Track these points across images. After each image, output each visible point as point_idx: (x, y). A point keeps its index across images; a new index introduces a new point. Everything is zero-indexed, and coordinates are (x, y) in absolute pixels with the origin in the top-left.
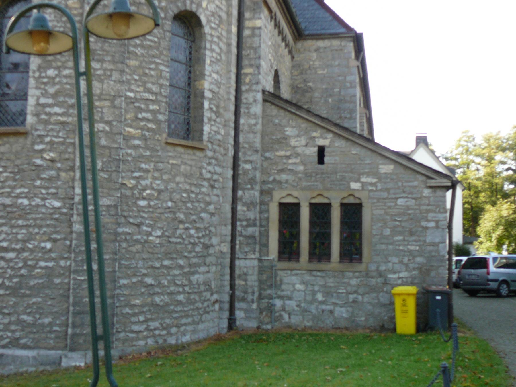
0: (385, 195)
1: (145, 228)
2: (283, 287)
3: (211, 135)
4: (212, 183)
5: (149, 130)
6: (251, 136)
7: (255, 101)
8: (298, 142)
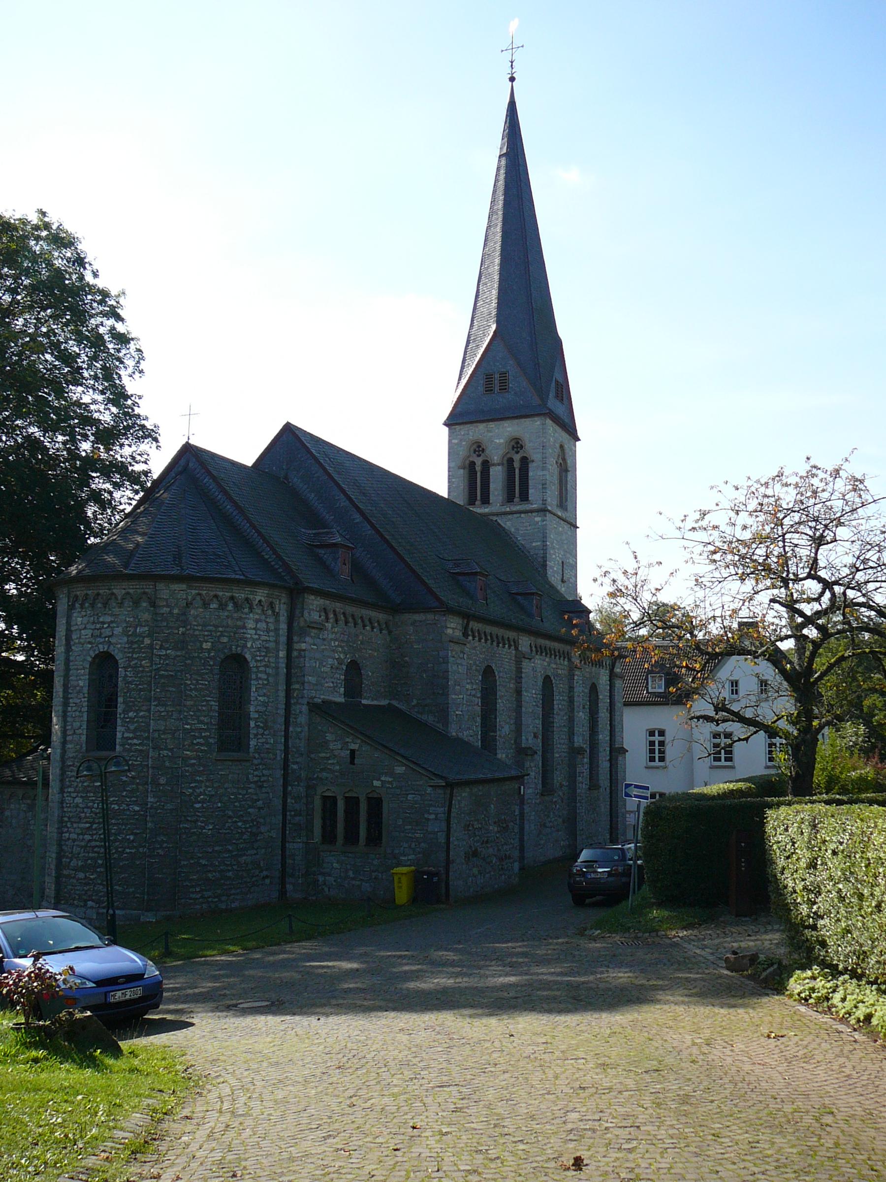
0: (398, 791)
2: (325, 865)
4: (260, 784)
6: (297, 741)
7: (301, 712)
8: (335, 746)
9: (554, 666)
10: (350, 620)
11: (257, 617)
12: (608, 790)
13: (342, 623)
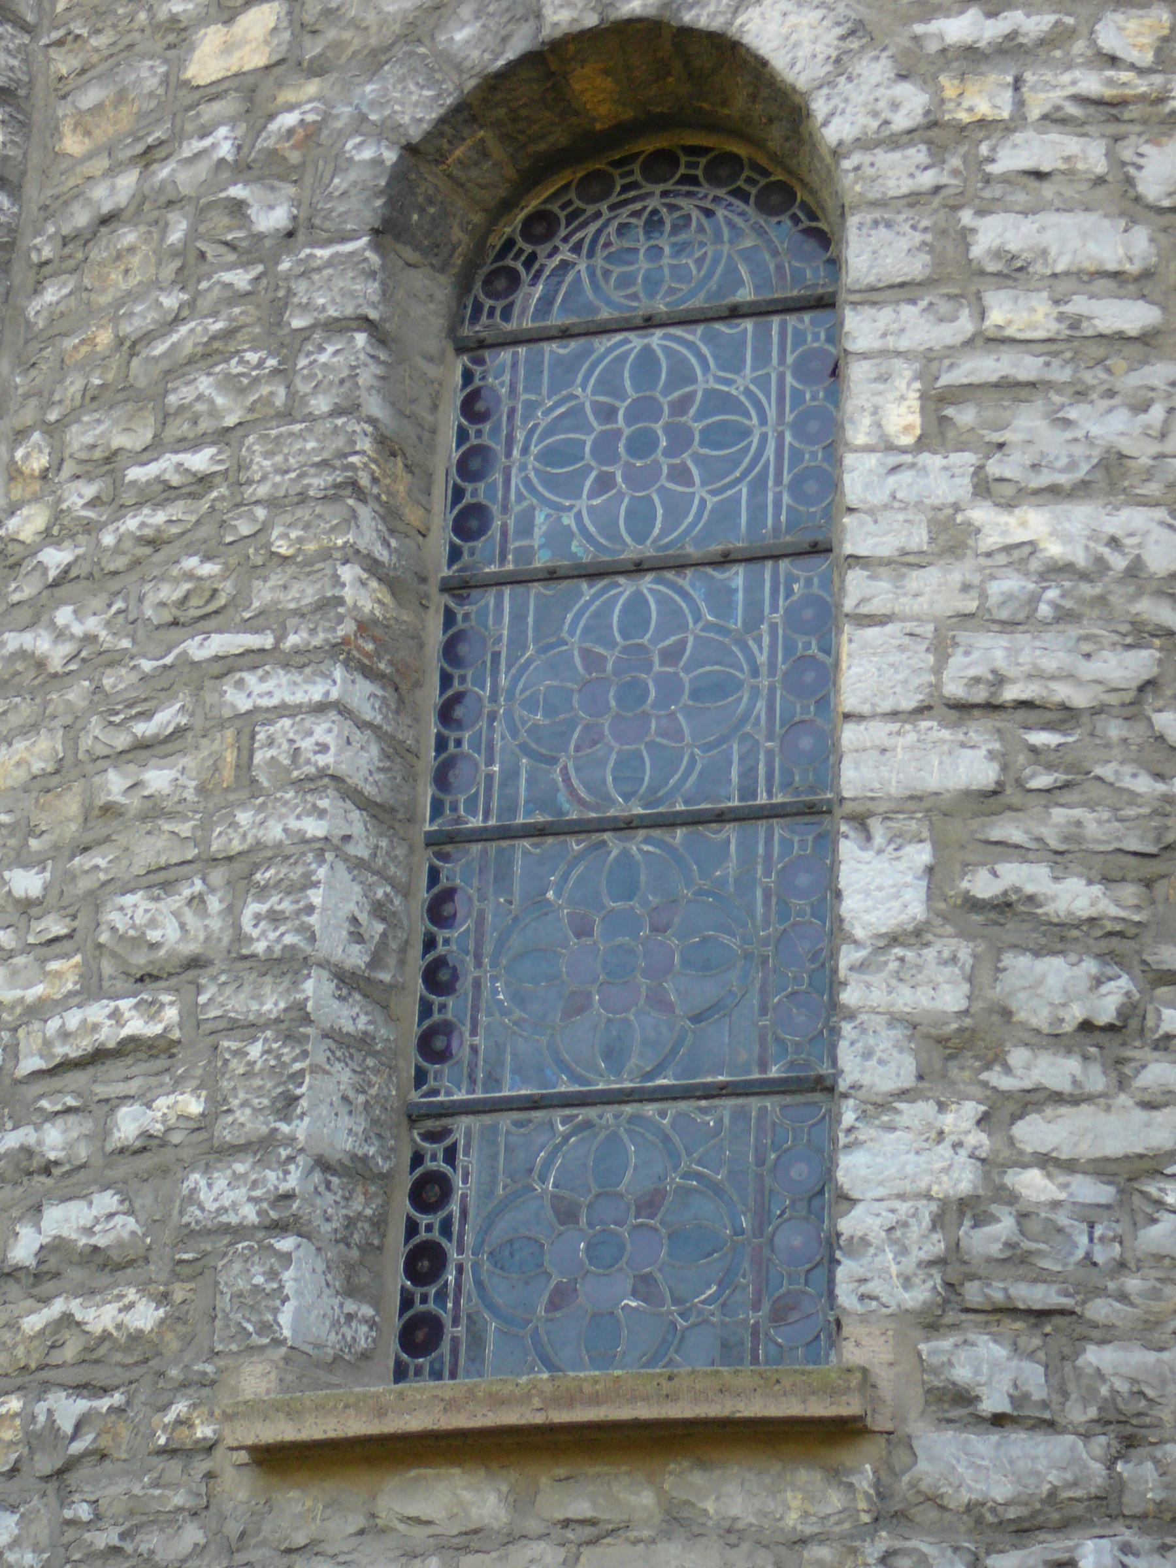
3: (989, 1239)
5: (94, 1366)
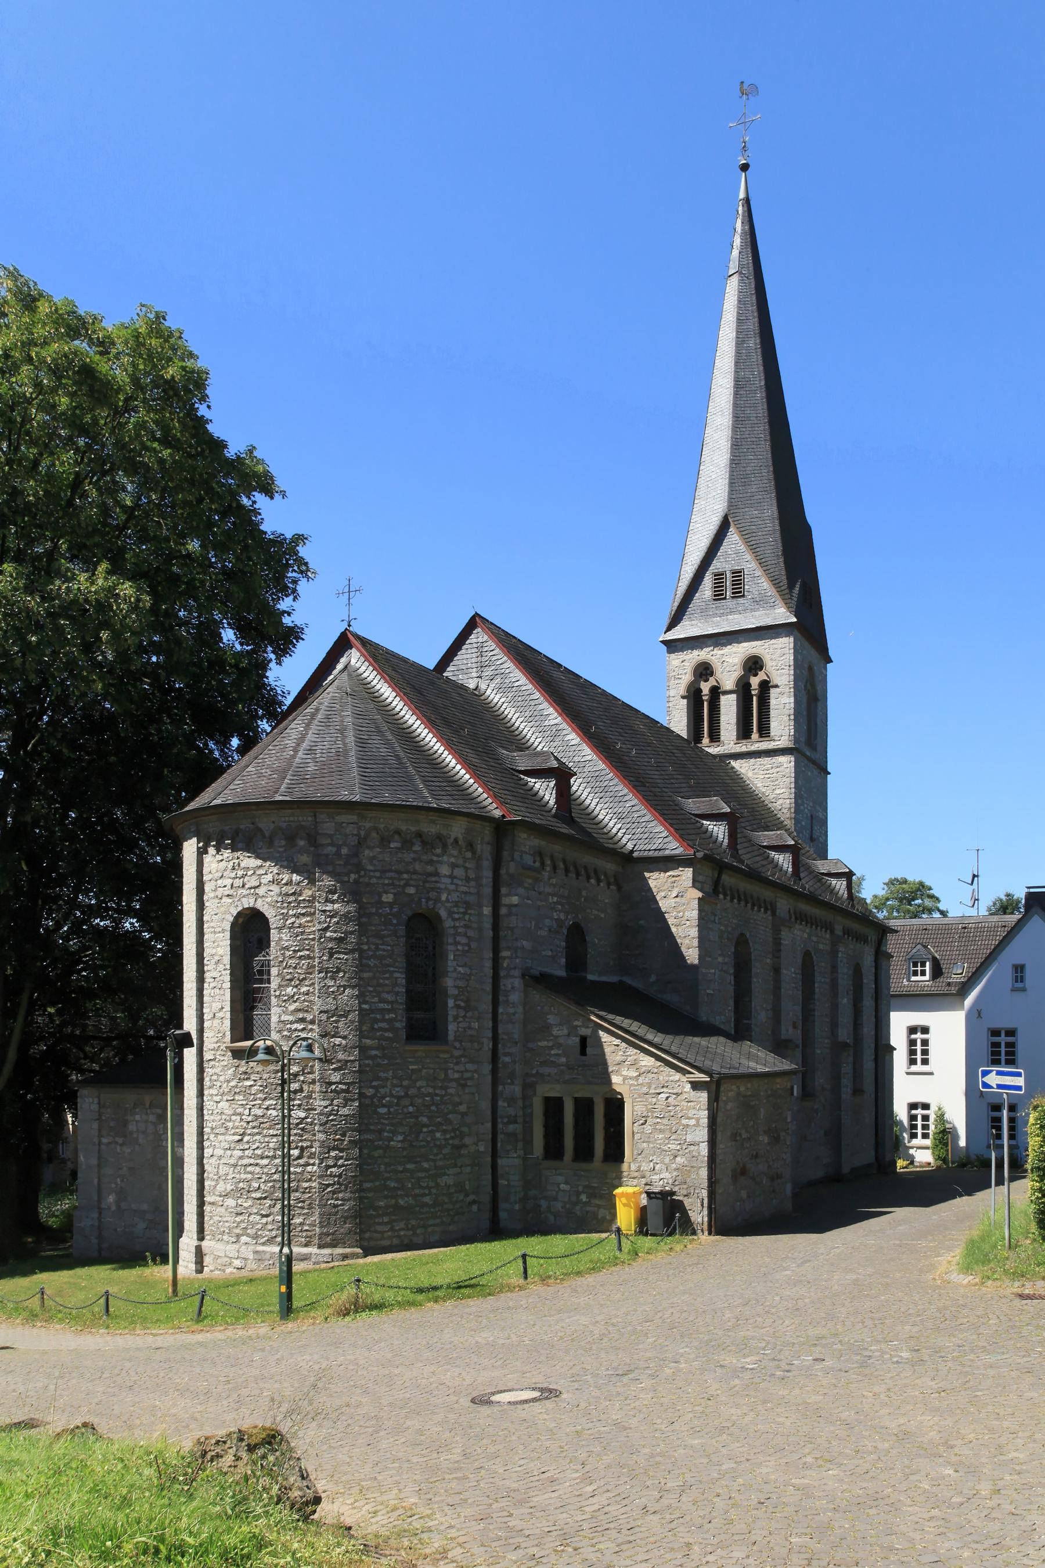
1: (386, 1134)
4: (463, 1082)
5: (387, 1039)
7: (513, 988)
9: (815, 939)
10: (572, 868)
11: (453, 860)
12: (873, 1096)
13: (561, 872)
